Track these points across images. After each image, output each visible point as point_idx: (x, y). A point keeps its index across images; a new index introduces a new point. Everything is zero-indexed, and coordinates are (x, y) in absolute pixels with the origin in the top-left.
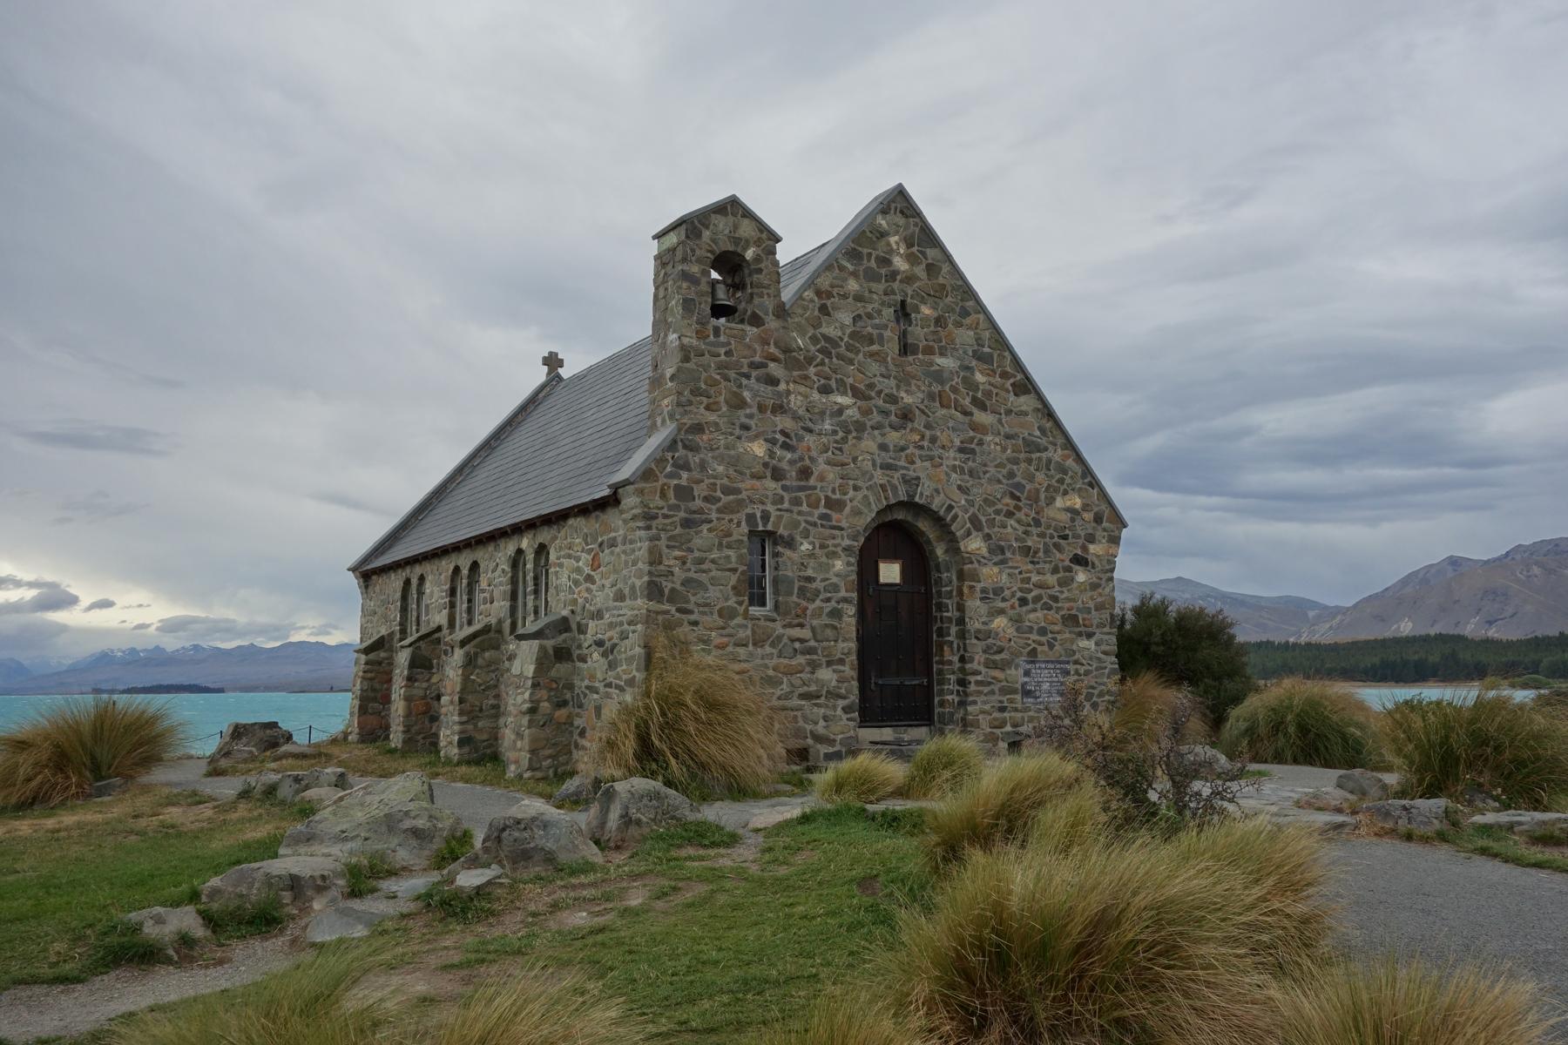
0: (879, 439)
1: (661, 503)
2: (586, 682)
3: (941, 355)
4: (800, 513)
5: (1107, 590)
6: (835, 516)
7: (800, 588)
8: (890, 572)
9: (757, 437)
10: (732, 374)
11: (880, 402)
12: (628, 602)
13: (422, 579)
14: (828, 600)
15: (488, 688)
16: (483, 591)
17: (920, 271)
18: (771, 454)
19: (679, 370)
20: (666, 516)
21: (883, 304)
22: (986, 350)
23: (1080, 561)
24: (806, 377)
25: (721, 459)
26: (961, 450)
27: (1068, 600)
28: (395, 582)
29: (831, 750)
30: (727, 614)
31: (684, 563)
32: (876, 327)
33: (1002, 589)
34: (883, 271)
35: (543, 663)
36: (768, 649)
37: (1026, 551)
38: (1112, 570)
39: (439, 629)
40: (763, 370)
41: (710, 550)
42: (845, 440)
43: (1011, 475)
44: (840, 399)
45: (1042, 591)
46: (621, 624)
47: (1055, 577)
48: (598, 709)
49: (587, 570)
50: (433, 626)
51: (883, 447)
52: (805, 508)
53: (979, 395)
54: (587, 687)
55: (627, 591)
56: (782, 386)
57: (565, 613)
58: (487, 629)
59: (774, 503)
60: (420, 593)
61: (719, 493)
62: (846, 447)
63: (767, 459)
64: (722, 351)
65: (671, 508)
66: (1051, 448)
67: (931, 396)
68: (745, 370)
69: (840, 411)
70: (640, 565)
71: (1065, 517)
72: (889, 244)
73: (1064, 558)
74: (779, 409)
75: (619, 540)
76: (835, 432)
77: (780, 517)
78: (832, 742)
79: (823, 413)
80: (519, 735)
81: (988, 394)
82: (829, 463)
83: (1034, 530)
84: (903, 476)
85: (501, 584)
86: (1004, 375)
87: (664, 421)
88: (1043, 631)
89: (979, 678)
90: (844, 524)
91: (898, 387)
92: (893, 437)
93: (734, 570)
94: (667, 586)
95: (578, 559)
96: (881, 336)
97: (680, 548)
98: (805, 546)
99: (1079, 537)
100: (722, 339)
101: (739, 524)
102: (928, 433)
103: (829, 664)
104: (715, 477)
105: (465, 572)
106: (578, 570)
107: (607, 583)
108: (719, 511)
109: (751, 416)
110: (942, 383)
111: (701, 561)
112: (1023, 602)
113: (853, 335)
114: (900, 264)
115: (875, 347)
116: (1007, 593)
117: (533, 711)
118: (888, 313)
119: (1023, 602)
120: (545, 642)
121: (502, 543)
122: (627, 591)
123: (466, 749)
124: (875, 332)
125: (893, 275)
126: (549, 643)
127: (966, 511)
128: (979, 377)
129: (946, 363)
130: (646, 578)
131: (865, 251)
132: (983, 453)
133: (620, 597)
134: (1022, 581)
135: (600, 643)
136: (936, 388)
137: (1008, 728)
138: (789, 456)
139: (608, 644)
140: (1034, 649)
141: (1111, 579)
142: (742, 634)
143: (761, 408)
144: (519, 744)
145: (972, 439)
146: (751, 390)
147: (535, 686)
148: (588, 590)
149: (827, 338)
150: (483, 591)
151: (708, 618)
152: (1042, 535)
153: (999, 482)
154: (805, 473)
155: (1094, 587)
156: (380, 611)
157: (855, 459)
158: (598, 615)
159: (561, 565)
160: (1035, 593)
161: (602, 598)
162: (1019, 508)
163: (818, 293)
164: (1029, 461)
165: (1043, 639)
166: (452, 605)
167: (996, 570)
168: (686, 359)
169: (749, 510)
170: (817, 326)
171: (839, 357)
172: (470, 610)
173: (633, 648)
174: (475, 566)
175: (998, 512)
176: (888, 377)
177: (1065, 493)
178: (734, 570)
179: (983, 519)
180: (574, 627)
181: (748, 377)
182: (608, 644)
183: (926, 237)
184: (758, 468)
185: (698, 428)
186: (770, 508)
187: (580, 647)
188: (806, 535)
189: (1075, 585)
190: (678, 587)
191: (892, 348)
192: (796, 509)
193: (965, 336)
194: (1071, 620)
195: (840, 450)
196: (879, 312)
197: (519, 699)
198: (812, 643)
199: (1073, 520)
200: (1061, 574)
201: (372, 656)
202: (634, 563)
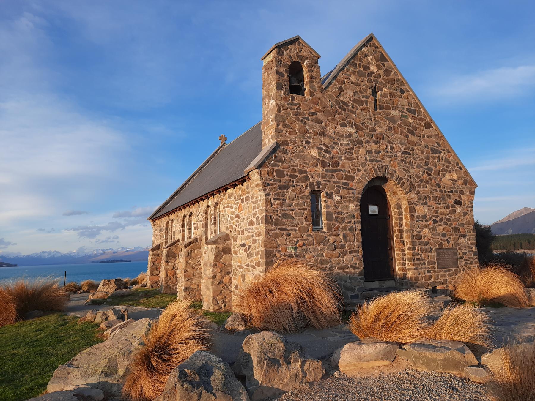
0: (368, 149)
1: (270, 178)
2: (237, 264)
3: (394, 109)
4: (334, 182)
5: (470, 215)
6: (350, 183)
7: (337, 218)
8: (373, 209)
9: (313, 147)
10: (301, 118)
11: (368, 131)
12: (255, 226)
13: (172, 220)
14: (349, 222)
15: (196, 266)
16: (194, 224)
17: (381, 72)
18: (320, 154)
19: (276, 116)
20: (272, 184)
21: (367, 87)
22: (413, 108)
23: (458, 202)
24: (334, 120)
25: (297, 157)
26: (404, 153)
27: (454, 220)
28: (163, 222)
29: (353, 294)
30: (304, 230)
31: (281, 206)
32: (363, 97)
33: (425, 216)
34: (366, 72)
35: (218, 256)
36: (322, 246)
37: (435, 198)
38: (472, 206)
39: (178, 241)
40: (315, 116)
41: (293, 200)
42: (352, 148)
43: (426, 164)
44: (351, 130)
45: (443, 217)
46: (253, 236)
47: (448, 210)
48: (243, 277)
49: (237, 212)
50: (176, 239)
51: (370, 152)
52: (336, 180)
53: (411, 128)
54: (238, 266)
55: (255, 220)
56: (323, 124)
57: (227, 232)
58: (196, 240)
59: (322, 178)
60: (172, 227)
61: (296, 174)
62: (353, 152)
63: (318, 157)
64: (295, 107)
65: (275, 180)
66: (443, 152)
67: (390, 129)
68: (307, 116)
69: (350, 135)
70: (261, 208)
71: (451, 182)
72: (368, 60)
73: (450, 202)
74: (323, 134)
75: (250, 197)
76: (348, 145)
77: (325, 185)
78: (354, 290)
79: (342, 136)
80: (208, 288)
81: (415, 128)
82: (347, 158)
83: (438, 189)
84: (379, 165)
85: (201, 221)
86: (421, 119)
87: (269, 141)
88: (444, 235)
89: (418, 257)
90: (354, 187)
91: (375, 124)
92: (374, 147)
93: (305, 209)
94: (274, 216)
95: (232, 208)
96: (366, 101)
97: (279, 199)
98: (337, 198)
99: (457, 192)
100: (296, 101)
101: (306, 188)
102: (389, 145)
103: (351, 252)
104: (295, 166)
105: (187, 217)
106: (233, 213)
107: (245, 217)
108: (297, 182)
109: (310, 137)
110: (394, 122)
111: (291, 205)
112: (435, 221)
113: (354, 101)
114: (373, 69)
115: (365, 106)
116: (428, 217)
117: (214, 277)
118: (369, 91)
119: (435, 221)
120: (218, 246)
121: (201, 203)
122: (255, 220)
123: (187, 293)
124: (364, 99)
125: (370, 74)
126: (220, 246)
127: (408, 181)
128: (410, 120)
129: (395, 113)
130: (264, 214)
131: (358, 63)
132: (413, 154)
133: (251, 224)
134: (434, 211)
135: (243, 245)
136: (392, 125)
137: (432, 280)
138: (328, 155)
139: (247, 246)
140: (441, 243)
141: (472, 211)
142: (310, 239)
143: (316, 134)
144: (208, 293)
145: (408, 148)
146: (309, 125)
147: (215, 265)
148: (237, 221)
149: (343, 102)
150: (194, 224)
151: (294, 232)
152: (441, 191)
153: (422, 167)
154: (336, 164)
155: (465, 214)
156: (158, 234)
157: (358, 157)
158: (243, 232)
159: (225, 211)
160: (441, 217)
161: (243, 225)
162: (431, 179)
163: (338, 81)
164: (434, 158)
165: (445, 238)
166: (183, 231)
167: (422, 207)
168: (279, 111)
169: (311, 181)
170: (338, 96)
171: (349, 110)
172: (189, 233)
173: (259, 247)
174: (191, 214)
175: (421, 181)
176: (371, 119)
177: (450, 172)
178: (305, 209)
179: (416, 184)
180: (232, 238)
181: (308, 119)
182: (247, 246)
183: (382, 58)
184: (315, 161)
185: (286, 143)
186: (320, 180)
187: (234, 247)
188: (337, 192)
189: (456, 214)
190: (278, 217)
191: (371, 107)
192: (332, 180)
193: (404, 102)
194: (456, 229)
195: (350, 153)
196: (365, 90)
197: (208, 272)
198: (343, 243)
199: (454, 184)
200: (451, 209)
201: (154, 252)
202: (258, 207)
